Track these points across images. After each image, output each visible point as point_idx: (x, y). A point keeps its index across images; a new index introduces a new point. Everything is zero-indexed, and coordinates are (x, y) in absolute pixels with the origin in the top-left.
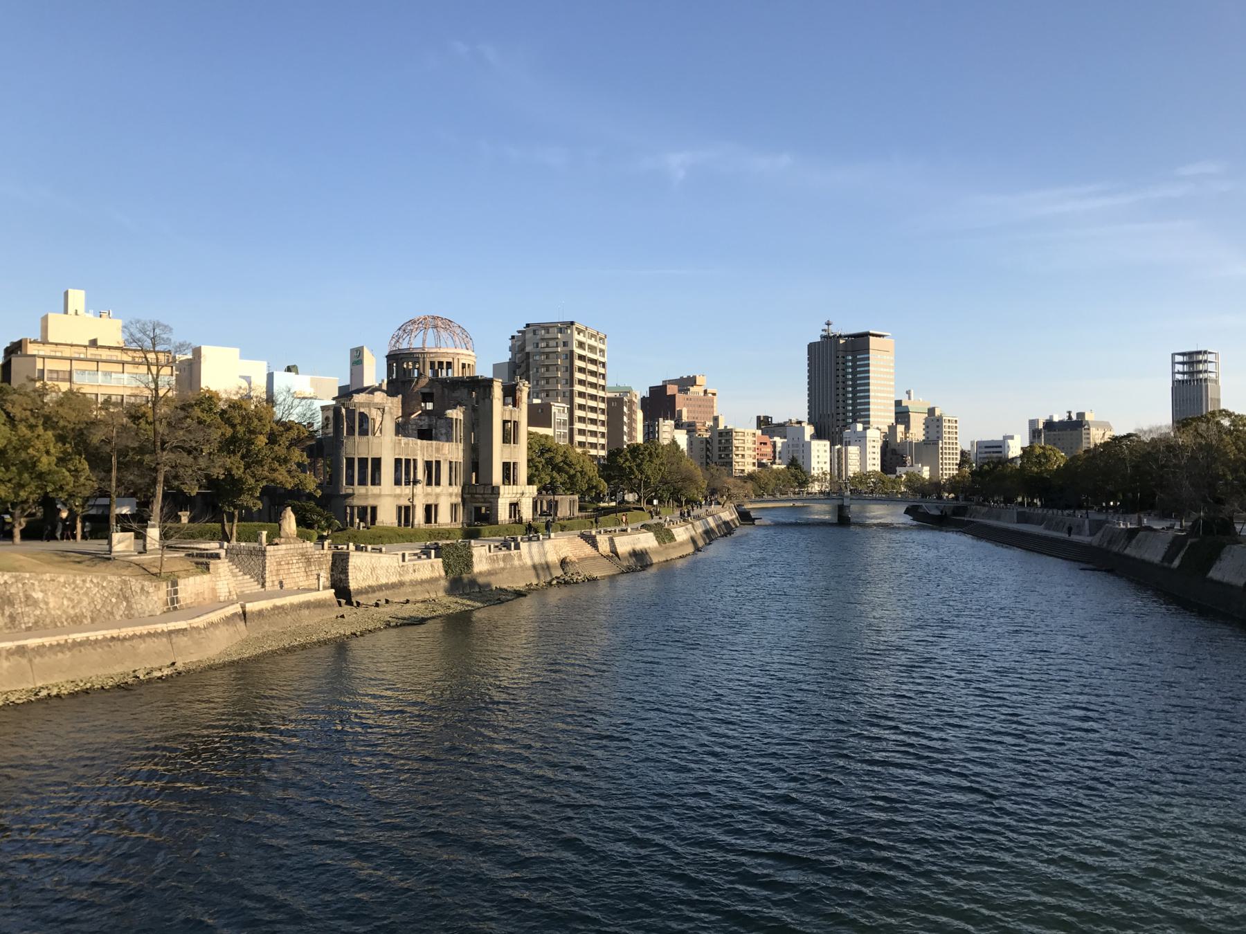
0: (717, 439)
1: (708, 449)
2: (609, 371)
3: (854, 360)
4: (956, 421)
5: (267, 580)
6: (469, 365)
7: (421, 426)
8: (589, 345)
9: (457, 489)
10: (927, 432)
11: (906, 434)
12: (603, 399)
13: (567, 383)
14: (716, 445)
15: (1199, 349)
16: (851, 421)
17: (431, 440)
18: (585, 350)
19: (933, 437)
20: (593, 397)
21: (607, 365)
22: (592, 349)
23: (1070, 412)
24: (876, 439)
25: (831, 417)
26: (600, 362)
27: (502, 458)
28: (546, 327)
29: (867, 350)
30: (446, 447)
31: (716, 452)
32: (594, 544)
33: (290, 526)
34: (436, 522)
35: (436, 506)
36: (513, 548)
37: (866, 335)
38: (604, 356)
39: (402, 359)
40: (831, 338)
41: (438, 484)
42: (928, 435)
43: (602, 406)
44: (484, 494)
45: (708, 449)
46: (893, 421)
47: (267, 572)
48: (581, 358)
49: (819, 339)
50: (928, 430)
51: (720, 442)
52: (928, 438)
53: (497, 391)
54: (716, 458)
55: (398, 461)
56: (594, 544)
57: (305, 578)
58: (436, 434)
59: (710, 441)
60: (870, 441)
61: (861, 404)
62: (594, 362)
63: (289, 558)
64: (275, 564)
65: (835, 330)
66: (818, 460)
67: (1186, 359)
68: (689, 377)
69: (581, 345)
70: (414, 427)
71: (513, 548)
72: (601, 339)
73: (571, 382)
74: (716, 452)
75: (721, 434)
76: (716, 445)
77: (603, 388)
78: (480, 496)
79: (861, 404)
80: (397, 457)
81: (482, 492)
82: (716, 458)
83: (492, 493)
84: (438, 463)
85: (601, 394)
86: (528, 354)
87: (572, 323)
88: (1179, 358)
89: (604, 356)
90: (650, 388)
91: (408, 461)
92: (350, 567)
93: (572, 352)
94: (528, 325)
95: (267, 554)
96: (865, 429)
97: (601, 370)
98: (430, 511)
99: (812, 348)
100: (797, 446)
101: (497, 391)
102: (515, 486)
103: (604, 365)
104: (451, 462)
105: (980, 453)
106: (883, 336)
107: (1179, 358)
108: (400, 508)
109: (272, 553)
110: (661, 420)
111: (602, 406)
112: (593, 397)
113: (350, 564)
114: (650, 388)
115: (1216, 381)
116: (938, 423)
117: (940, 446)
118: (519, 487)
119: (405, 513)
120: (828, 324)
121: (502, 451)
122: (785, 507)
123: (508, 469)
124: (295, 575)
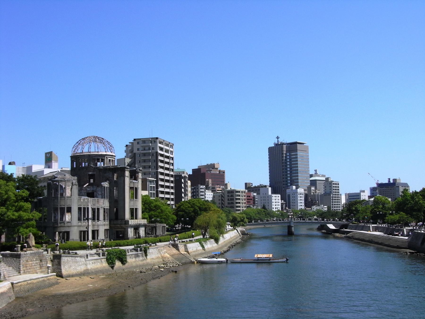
0: (226, 194)
1: (222, 200)
2: (175, 162)
3: (290, 155)
4: (338, 184)
5: (21, 269)
6: (112, 160)
7: (89, 191)
8: (165, 149)
9: (107, 222)
10: (326, 190)
11: (315, 190)
12: (172, 176)
13: (154, 168)
14: (226, 198)
16: (289, 184)
17: (94, 197)
18: (163, 151)
19: (328, 191)
20: (168, 175)
21: (174, 159)
22: (167, 151)
23: (389, 179)
24: (302, 193)
25: (280, 183)
26: (171, 157)
27: (130, 206)
28: (144, 141)
29: (296, 150)
30: (101, 201)
31: (226, 202)
32: (178, 249)
33: (32, 243)
34: (97, 239)
35: (98, 231)
36: (139, 251)
37: (296, 143)
38: (172, 154)
39: (78, 158)
40: (279, 145)
41: (98, 219)
42: (326, 191)
43: (172, 179)
44: (121, 224)
46: (309, 184)
47: (21, 265)
48: (162, 155)
49: (274, 146)
50: (325, 188)
51: (228, 196)
52: (326, 192)
53: (127, 173)
54: (226, 204)
55: (80, 209)
56: (178, 249)
57: (40, 268)
58: (96, 195)
59: (223, 196)
60: (299, 194)
61: (294, 176)
62: (168, 157)
63: (32, 258)
64: (25, 261)
65: (281, 140)
66: (275, 204)
68: (211, 164)
69: (161, 149)
70: (85, 191)
71: (139, 251)
72: (171, 146)
73: (157, 167)
74: (226, 202)
75: (229, 192)
76: (226, 198)
77: (173, 170)
78: (119, 225)
79: (294, 176)
80: (79, 206)
81: (120, 223)
82: (226, 204)
83: (125, 224)
84: (98, 209)
85: (172, 173)
86: (135, 154)
87: (157, 138)
89: (172, 154)
91: (84, 208)
92: (62, 262)
93: (157, 152)
94: (135, 140)
95: (21, 256)
96: (297, 188)
97: (171, 161)
98: (95, 233)
99: (270, 149)
100: (265, 197)
101: (127, 173)
102: (136, 220)
103: (172, 159)
104: (104, 209)
105: (350, 199)
106: (304, 144)
108: (81, 232)
109: (24, 256)
110: (199, 185)
111: (172, 179)
112: (168, 175)
113: (62, 260)
114: (193, 170)
116: (330, 185)
117: (332, 196)
118: (138, 220)
119: (84, 235)
121: (130, 203)
122: (261, 228)
123: (133, 213)
124: (35, 267)
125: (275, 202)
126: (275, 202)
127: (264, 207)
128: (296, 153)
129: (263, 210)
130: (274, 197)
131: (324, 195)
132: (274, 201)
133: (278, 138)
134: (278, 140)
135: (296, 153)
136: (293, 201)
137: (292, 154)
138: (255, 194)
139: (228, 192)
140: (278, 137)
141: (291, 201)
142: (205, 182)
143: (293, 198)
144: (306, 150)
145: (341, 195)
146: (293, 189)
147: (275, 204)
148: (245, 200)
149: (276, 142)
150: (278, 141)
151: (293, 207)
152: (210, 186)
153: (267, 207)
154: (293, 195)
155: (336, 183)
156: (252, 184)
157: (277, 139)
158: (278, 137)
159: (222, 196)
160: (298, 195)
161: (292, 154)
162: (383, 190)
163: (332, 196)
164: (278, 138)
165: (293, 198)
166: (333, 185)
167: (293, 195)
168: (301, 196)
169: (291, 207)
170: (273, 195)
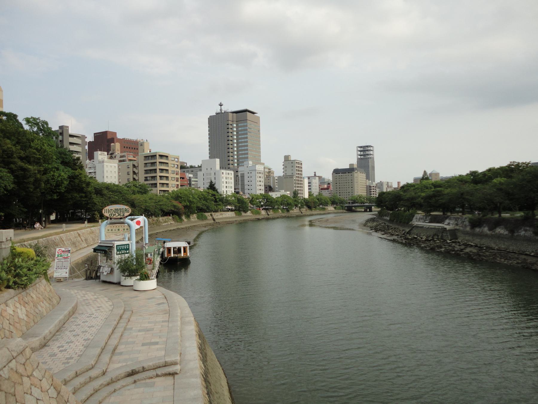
1: (134, 173)
15: (367, 145)
19: (289, 173)
24: (262, 172)
45: (134, 173)
52: (286, 174)
59: (136, 165)
66: (226, 185)
67: (361, 149)
88: (359, 149)
90: (95, 134)
106: (253, 113)
107: (359, 149)
114: (95, 134)
115: (373, 158)
120: (221, 105)
125: (226, 182)
126: (226, 182)
127: (212, 187)
128: (245, 124)
129: (211, 191)
130: (224, 173)
131: (284, 178)
132: (224, 180)
133: (221, 105)
134: (221, 107)
135: (245, 124)
136: (249, 183)
137: (239, 125)
138: (191, 176)
139: (145, 157)
140: (221, 103)
141: (246, 182)
142: (110, 146)
143: (249, 179)
144: (257, 122)
145: (304, 177)
146: (250, 165)
147: (226, 185)
148: (177, 181)
149: (219, 111)
150: (221, 110)
151: (250, 192)
152: (116, 153)
153: (217, 186)
154: (249, 175)
155: (299, 162)
156: (186, 163)
157: (220, 106)
158: (221, 103)
159: (134, 166)
160: (257, 174)
161: (239, 125)
162: (339, 176)
163: (294, 179)
164: (221, 105)
165: (249, 179)
166: (296, 165)
167: (249, 175)
168: (260, 175)
169: (246, 191)
170: (222, 171)
